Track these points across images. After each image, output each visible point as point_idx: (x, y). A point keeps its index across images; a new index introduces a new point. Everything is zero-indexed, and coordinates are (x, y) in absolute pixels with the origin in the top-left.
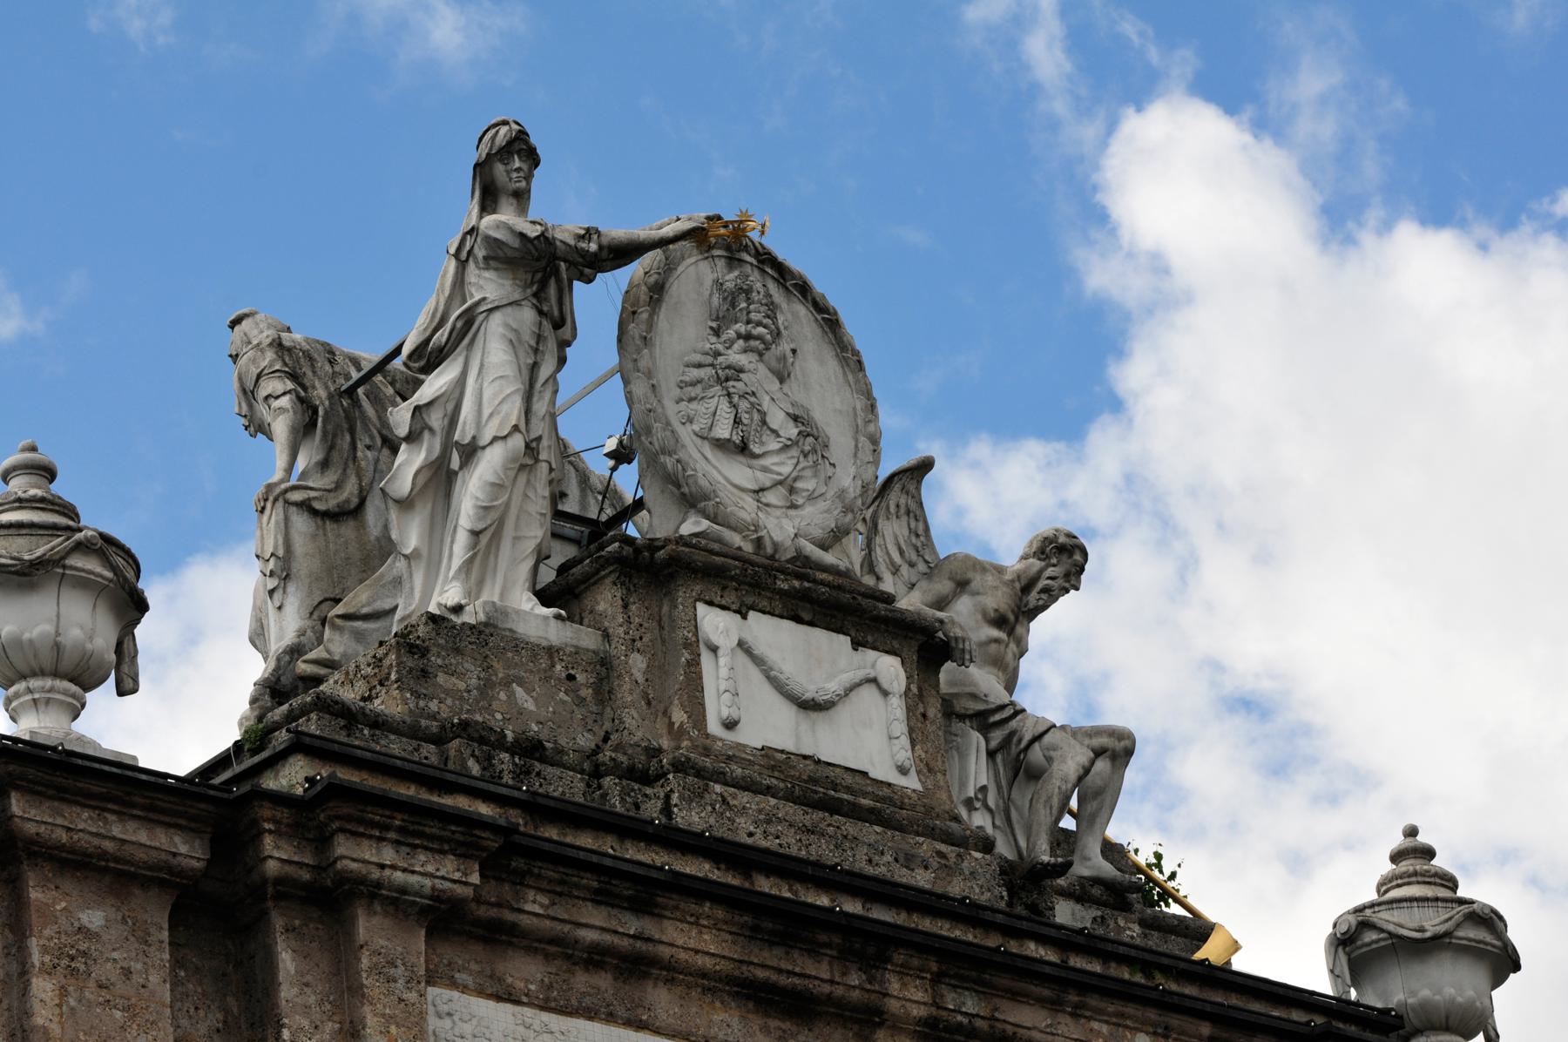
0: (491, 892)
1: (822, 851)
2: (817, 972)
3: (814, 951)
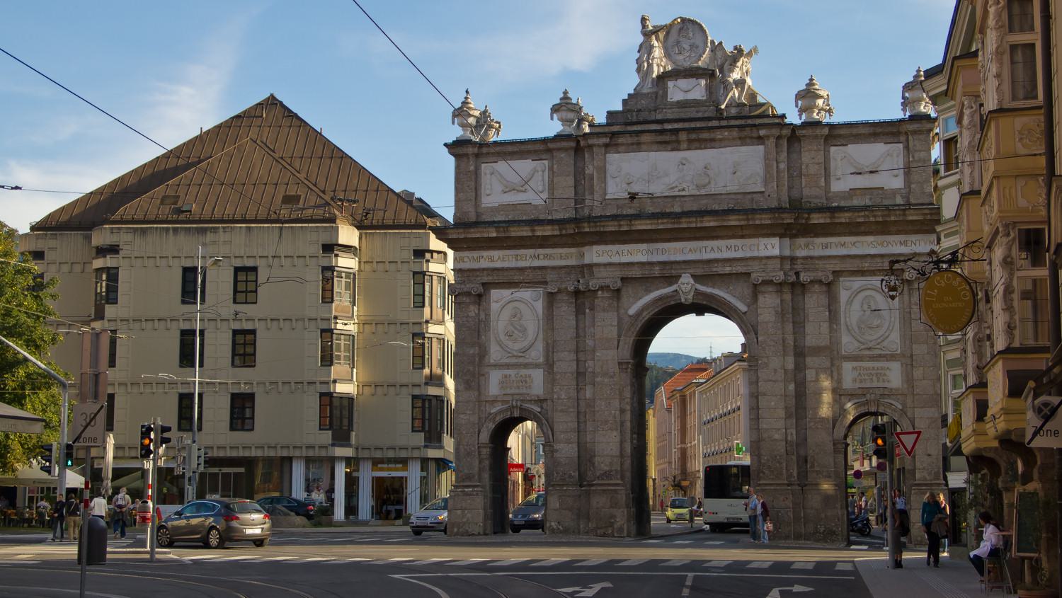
0: (613, 140)
1: (683, 116)
2: (667, 138)
3: (666, 135)
